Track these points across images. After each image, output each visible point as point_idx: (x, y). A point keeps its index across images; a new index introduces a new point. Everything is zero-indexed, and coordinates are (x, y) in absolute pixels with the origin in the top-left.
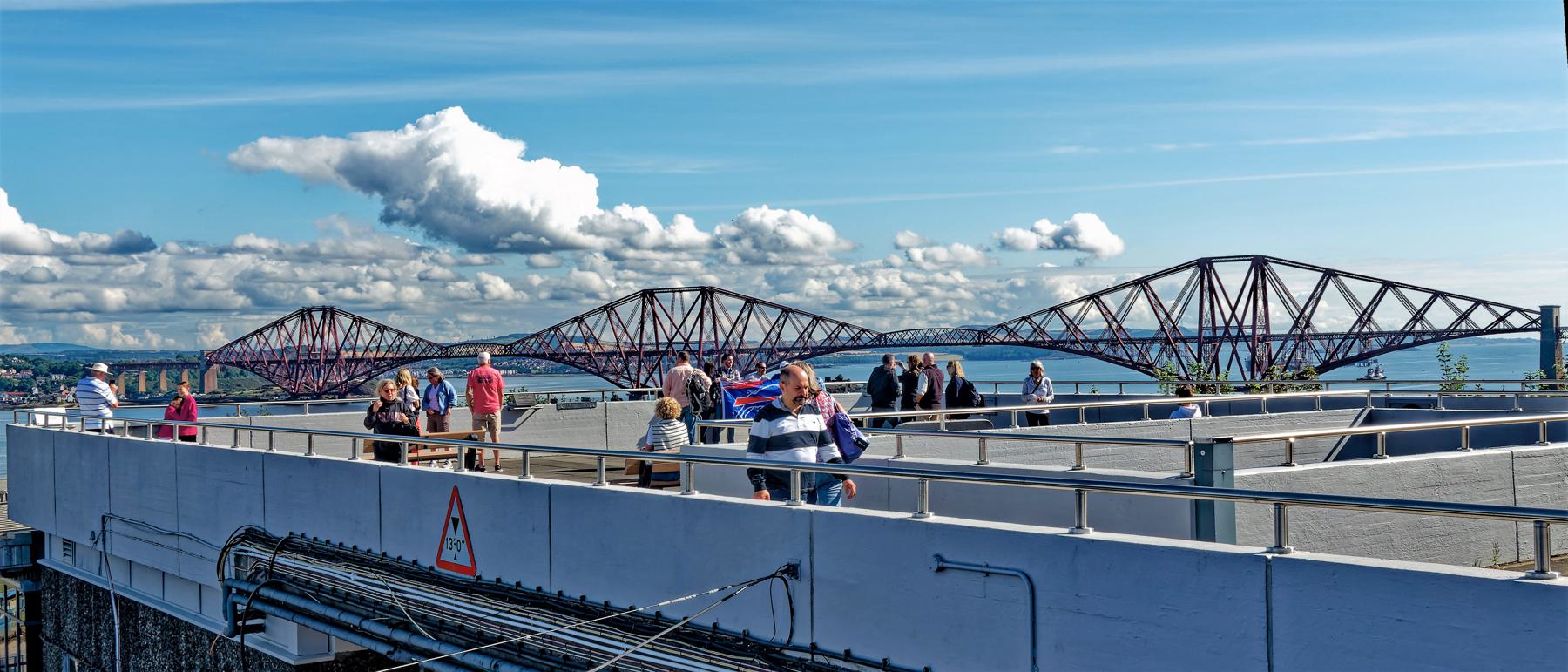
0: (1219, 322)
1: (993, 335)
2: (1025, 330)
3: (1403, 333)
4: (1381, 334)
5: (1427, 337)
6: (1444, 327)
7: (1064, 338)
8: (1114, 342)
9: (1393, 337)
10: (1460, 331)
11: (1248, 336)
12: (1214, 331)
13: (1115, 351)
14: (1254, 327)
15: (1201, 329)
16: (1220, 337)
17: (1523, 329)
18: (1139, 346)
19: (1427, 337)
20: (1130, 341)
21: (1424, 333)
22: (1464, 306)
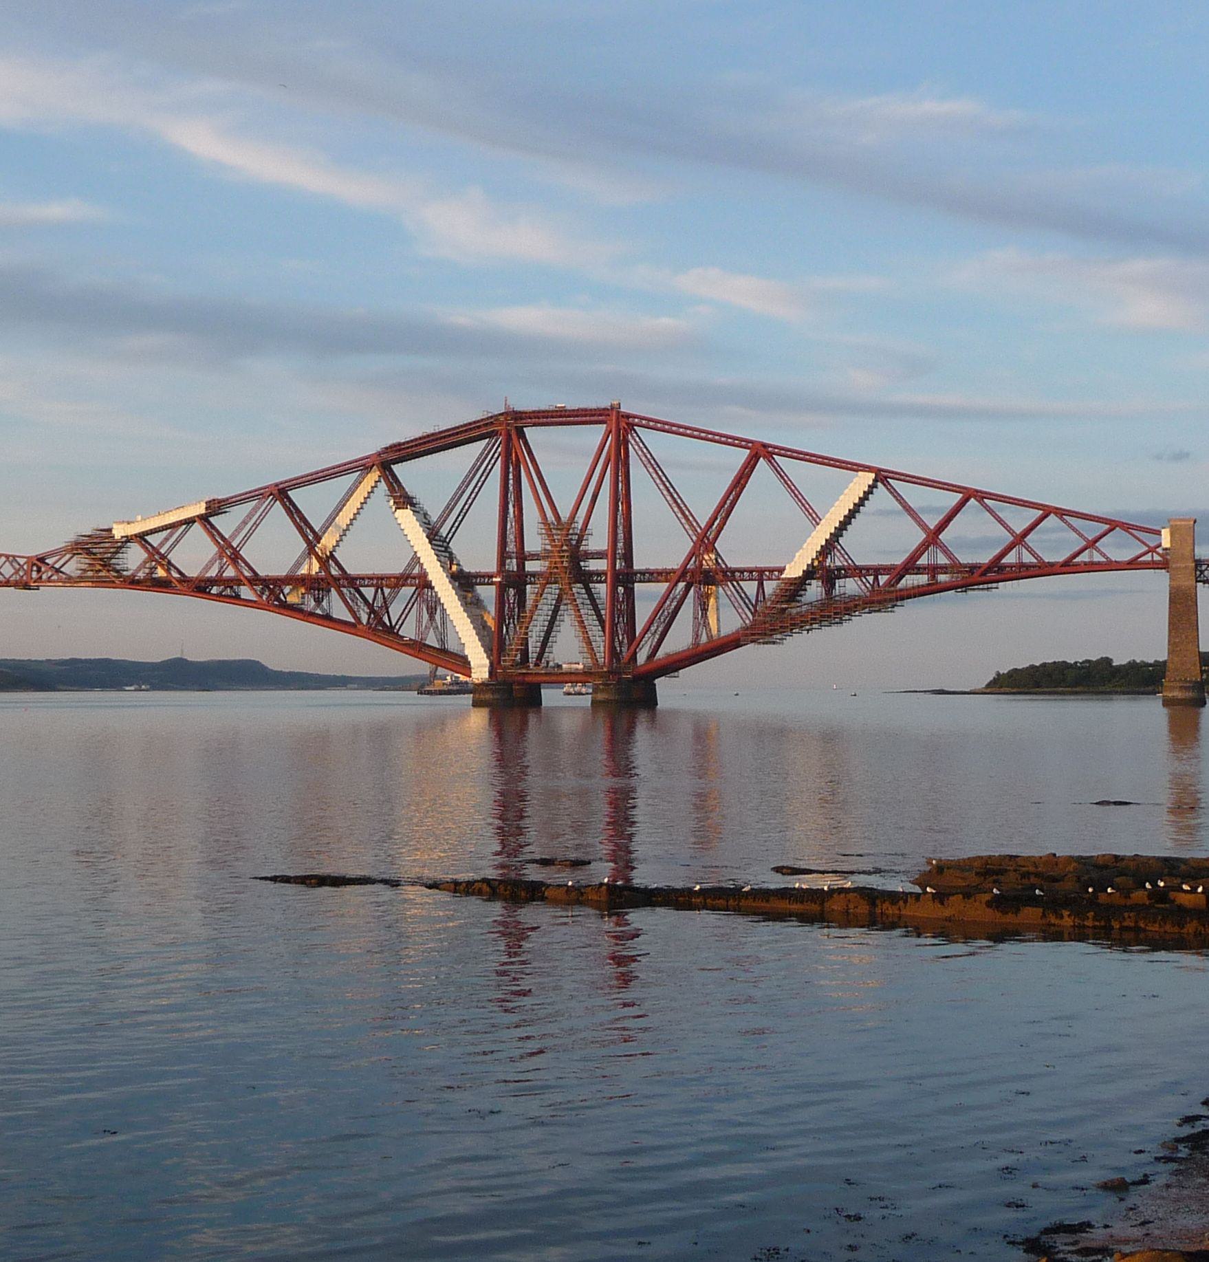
0: (534, 541)
1: (57, 566)
2: (134, 558)
3: (910, 566)
4: (858, 571)
5: (942, 578)
6: (985, 558)
7: (213, 573)
8: (317, 586)
9: (883, 579)
10: (1011, 566)
11: (599, 574)
12: (521, 566)
13: (318, 601)
14: (611, 554)
15: (503, 556)
16: (533, 575)
17: (1133, 564)
18: (369, 592)
19: (942, 578)
20: (354, 582)
21: (943, 569)
22: (1020, 520)
